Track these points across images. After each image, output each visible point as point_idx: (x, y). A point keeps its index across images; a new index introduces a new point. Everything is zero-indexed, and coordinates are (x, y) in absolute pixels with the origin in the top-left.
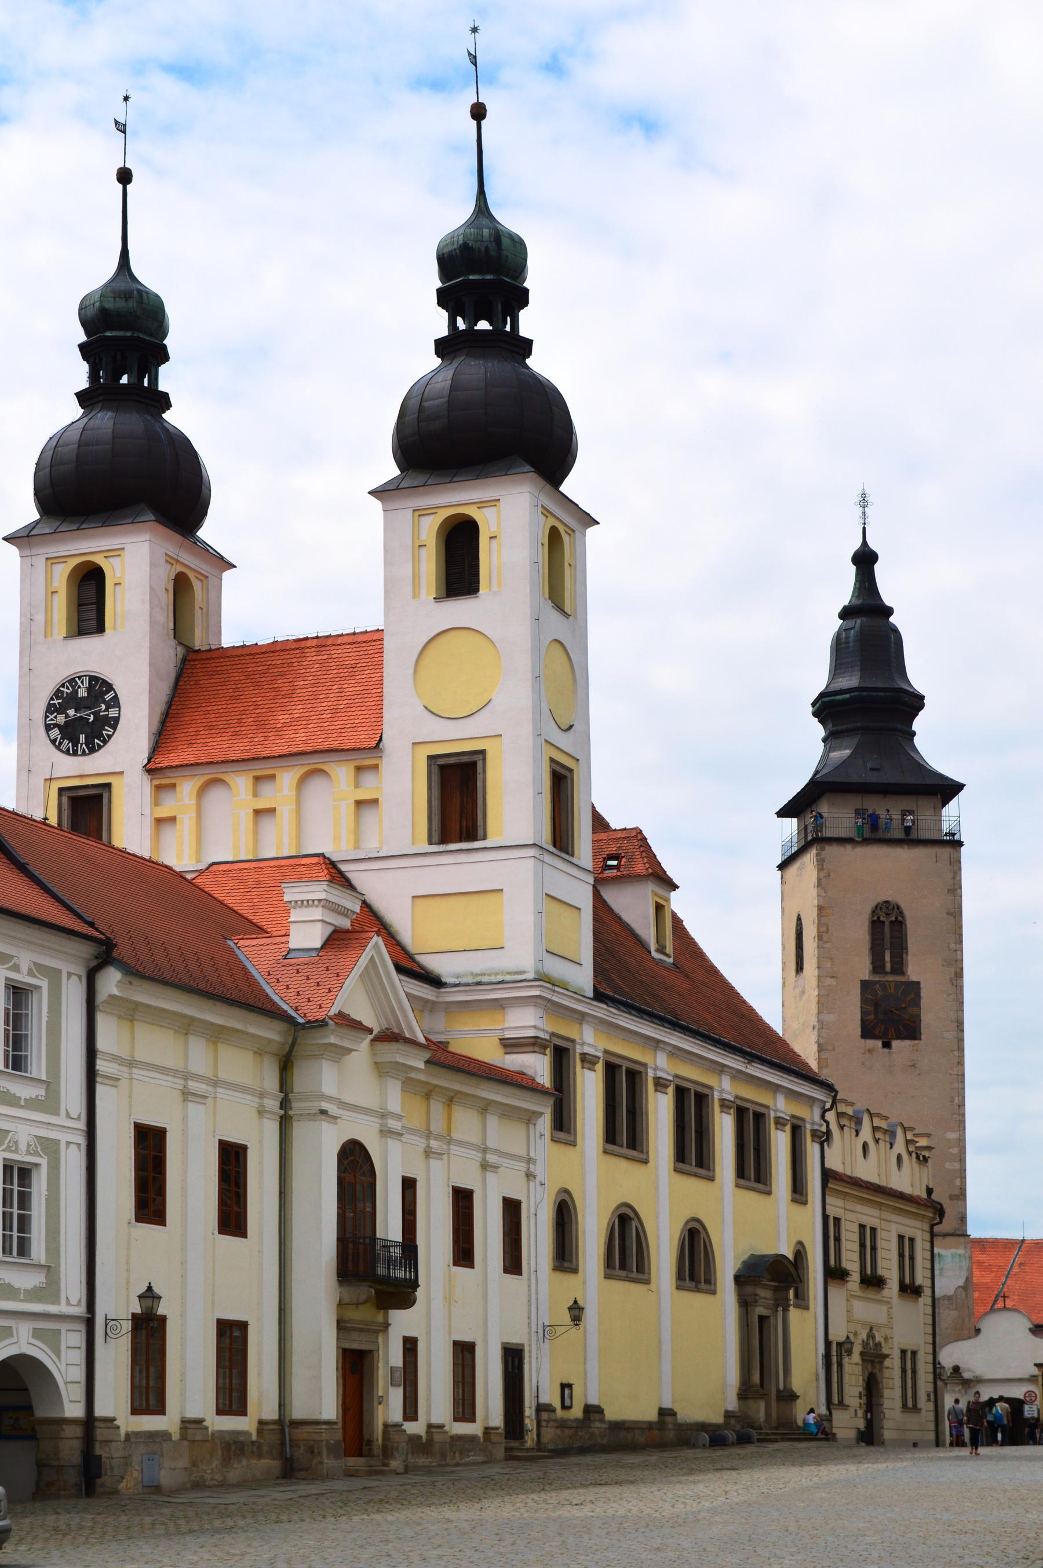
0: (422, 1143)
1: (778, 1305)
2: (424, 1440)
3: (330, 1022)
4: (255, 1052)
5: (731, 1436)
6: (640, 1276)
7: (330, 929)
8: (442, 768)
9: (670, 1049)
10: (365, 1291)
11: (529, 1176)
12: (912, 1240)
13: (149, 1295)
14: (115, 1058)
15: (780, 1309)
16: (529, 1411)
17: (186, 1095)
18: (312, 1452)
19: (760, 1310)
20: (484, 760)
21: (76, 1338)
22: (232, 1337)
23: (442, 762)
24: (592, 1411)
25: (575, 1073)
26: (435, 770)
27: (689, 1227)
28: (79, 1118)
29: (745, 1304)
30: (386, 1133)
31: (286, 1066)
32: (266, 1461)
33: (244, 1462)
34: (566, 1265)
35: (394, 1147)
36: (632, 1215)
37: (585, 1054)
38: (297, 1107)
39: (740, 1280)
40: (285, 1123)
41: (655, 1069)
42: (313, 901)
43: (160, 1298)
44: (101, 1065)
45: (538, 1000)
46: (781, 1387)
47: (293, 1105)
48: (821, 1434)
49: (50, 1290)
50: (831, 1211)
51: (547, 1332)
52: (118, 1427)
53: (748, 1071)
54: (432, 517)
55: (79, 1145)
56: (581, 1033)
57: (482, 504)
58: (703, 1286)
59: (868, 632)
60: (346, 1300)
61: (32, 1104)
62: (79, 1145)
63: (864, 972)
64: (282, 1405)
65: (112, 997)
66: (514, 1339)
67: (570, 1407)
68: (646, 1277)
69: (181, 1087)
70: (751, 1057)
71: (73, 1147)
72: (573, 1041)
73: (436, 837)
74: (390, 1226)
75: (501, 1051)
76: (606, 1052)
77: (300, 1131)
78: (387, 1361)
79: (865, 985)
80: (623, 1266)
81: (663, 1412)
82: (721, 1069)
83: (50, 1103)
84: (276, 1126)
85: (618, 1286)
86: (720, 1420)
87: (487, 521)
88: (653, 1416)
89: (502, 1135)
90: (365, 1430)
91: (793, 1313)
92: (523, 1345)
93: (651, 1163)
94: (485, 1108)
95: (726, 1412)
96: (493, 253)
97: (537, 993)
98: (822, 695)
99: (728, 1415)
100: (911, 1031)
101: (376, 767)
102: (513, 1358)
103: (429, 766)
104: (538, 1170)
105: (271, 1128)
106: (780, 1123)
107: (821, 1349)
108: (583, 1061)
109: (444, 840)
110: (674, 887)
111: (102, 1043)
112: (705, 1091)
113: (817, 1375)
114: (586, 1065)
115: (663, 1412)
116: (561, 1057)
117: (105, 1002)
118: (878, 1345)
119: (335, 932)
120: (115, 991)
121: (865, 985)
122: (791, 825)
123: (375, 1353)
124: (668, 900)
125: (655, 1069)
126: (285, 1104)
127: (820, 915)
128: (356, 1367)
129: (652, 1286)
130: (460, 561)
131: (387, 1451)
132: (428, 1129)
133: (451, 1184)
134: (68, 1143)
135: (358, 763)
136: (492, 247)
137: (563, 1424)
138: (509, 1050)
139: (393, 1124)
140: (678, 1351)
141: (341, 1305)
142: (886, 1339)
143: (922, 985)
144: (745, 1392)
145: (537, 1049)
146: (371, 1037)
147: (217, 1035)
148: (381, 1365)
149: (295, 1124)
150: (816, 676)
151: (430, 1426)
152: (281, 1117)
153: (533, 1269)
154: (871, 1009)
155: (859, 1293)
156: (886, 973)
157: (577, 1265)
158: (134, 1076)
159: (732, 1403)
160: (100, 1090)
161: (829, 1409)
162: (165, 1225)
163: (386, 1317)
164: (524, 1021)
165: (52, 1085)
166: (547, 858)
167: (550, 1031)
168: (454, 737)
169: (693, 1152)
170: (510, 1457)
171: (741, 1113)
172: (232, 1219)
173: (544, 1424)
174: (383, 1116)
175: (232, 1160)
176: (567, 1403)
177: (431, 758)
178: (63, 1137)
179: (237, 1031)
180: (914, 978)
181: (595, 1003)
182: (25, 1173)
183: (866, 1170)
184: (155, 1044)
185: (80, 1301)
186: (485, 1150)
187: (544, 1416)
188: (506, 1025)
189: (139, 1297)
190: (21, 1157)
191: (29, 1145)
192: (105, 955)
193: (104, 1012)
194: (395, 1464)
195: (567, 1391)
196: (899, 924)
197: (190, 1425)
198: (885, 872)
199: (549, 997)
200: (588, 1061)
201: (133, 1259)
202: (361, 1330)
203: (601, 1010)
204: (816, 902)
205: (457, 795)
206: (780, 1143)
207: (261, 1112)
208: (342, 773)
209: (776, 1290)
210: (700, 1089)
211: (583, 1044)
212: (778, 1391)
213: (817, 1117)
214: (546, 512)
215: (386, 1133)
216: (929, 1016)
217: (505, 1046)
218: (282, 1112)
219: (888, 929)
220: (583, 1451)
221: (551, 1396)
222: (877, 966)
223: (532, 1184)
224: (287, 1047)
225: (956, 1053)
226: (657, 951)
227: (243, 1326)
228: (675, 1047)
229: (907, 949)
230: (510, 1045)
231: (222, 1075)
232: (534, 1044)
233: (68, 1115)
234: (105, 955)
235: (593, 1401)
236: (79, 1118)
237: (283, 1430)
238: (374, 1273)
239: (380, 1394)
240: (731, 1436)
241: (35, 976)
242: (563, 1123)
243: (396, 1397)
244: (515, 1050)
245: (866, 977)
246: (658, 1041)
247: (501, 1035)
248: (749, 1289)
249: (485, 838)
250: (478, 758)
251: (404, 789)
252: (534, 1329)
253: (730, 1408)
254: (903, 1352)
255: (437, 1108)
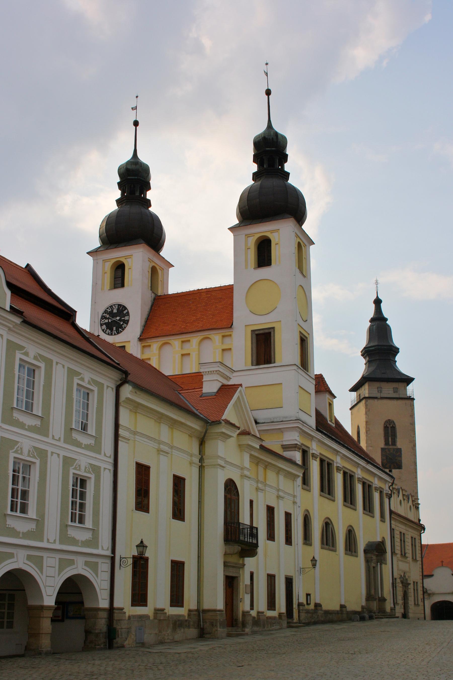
0: (255, 485)
1: (378, 562)
2: (256, 619)
3: (223, 422)
4: (189, 436)
5: (367, 615)
6: (333, 548)
7: (221, 384)
8: (257, 335)
9: (341, 455)
10: (237, 548)
11: (294, 503)
12: (415, 539)
13: (142, 545)
14: (128, 429)
15: (379, 564)
16: (295, 606)
17: (159, 451)
18: (213, 625)
19: (373, 565)
20: (274, 331)
21: (105, 566)
22: (177, 568)
23: (257, 332)
24: (317, 606)
25: (310, 461)
26: (254, 336)
27: (349, 529)
28: (110, 457)
29: (367, 561)
30: (243, 476)
31: (202, 443)
32: (192, 629)
33: (182, 630)
34: (308, 542)
35: (247, 483)
36: (330, 523)
37: (314, 453)
38: (207, 462)
39: (366, 551)
40: (201, 468)
41: (337, 463)
42: (213, 371)
43: (147, 547)
44: (121, 432)
45: (297, 429)
46: (380, 596)
47: (205, 461)
48: (392, 616)
49: (94, 542)
50: (393, 526)
51: (302, 570)
52: (125, 613)
53: (367, 467)
54: (252, 237)
55: (110, 470)
56: (312, 445)
57: (272, 232)
58: (353, 553)
59: (379, 326)
60: (228, 552)
61: (88, 447)
62: (110, 470)
63: (382, 445)
64: (199, 602)
65: (128, 399)
66: (289, 574)
67: (310, 604)
68: (335, 549)
69: (157, 447)
70: (368, 462)
71: (107, 471)
72: (309, 448)
73: (255, 363)
74: (245, 519)
75: (282, 450)
76: (320, 454)
77: (208, 472)
78: (244, 582)
79: (382, 449)
80: (327, 544)
81: (342, 606)
82: (358, 465)
83: (96, 448)
84: (197, 470)
85: (326, 552)
86: (359, 609)
87: (274, 238)
88: (338, 608)
89: (285, 484)
90: (234, 615)
91: (383, 565)
92: (292, 576)
93: (336, 502)
94: (279, 471)
95: (362, 606)
96: (275, 140)
97: (297, 425)
98: (365, 348)
99: (363, 607)
100: (399, 467)
101: (230, 335)
102: (289, 582)
103: (252, 334)
104: (298, 500)
105: (195, 471)
106: (376, 489)
107: (391, 581)
108: (313, 456)
109: (258, 364)
110: (335, 397)
111: (121, 422)
112: (353, 474)
113: (390, 591)
114: (314, 458)
115: (342, 606)
116: (305, 453)
117: (123, 401)
118: (407, 580)
119: (222, 386)
120: (129, 396)
121: (382, 449)
122: (354, 394)
123: (239, 578)
124: (333, 402)
125: (337, 463)
126: (201, 460)
127: (366, 425)
128: (231, 583)
129: (337, 553)
130: (264, 254)
131: (244, 625)
132: (257, 478)
133: (266, 504)
134: (105, 469)
135: (223, 334)
136: (275, 138)
137: (308, 612)
138: (285, 450)
139: (246, 473)
140: (337, 581)
141: (226, 554)
142: (409, 577)
143: (402, 449)
144: (369, 597)
145: (296, 449)
146: (238, 431)
147: (173, 424)
148: (241, 584)
149: (206, 470)
150: (362, 341)
151: (258, 612)
152: (200, 467)
153: (296, 543)
154: (385, 458)
155: (400, 559)
156: (390, 445)
157: (312, 543)
158: (136, 439)
159: (364, 603)
160: (121, 444)
161: (394, 605)
162: (149, 513)
163: (243, 561)
164: (293, 437)
165: (98, 438)
166: (300, 371)
167: (301, 442)
168: (262, 323)
169: (349, 499)
170: (290, 626)
171: (364, 484)
172: (178, 513)
173: (301, 611)
174: (242, 469)
175: (179, 483)
176: (309, 602)
177: (253, 331)
178: (103, 465)
179: (182, 423)
180: (399, 447)
181: (317, 432)
182: (83, 482)
183: (401, 511)
184: (145, 425)
185: (108, 548)
186: (278, 490)
187: (301, 608)
188: (284, 439)
189: (137, 546)
190: (82, 473)
191: (86, 468)
192: (125, 378)
193: (123, 406)
194: (247, 630)
195: (309, 597)
196: (394, 428)
197: (158, 611)
198: (389, 410)
199: (301, 427)
200: (314, 456)
201: (134, 528)
202: (233, 567)
203: (319, 436)
204: (365, 420)
205: (263, 346)
206: (376, 496)
207: (191, 463)
208: (216, 337)
209: (377, 556)
210: (351, 473)
211: (312, 449)
212: (379, 597)
213: (387, 489)
214: (297, 236)
215: (243, 476)
216: (405, 460)
217: (283, 448)
218: (200, 464)
219: (390, 430)
220: (315, 623)
221: (303, 600)
222: (387, 443)
223: (295, 507)
224: (203, 434)
225: (414, 474)
226: (330, 421)
227: (183, 563)
228: (344, 455)
229: (396, 436)
230: (285, 448)
231: (175, 444)
232: (295, 447)
233: (105, 455)
234: (125, 378)
235: (318, 601)
236: (110, 457)
237: (199, 614)
238: (240, 541)
239: (241, 597)
240: (367, 615)
241: (91, 385)
242: (306, 481)
243: (247, 598)
244: (288, 450)
245: (383, 447)
246: (338, 452)
247: (282, 443)
248: (369, 555)
249: (274, 362)
250: (271, 331)
251: (241, 344)
252: (297, 569)
253: (363, 605)
254: (414, 582)
255: (261, 469)
